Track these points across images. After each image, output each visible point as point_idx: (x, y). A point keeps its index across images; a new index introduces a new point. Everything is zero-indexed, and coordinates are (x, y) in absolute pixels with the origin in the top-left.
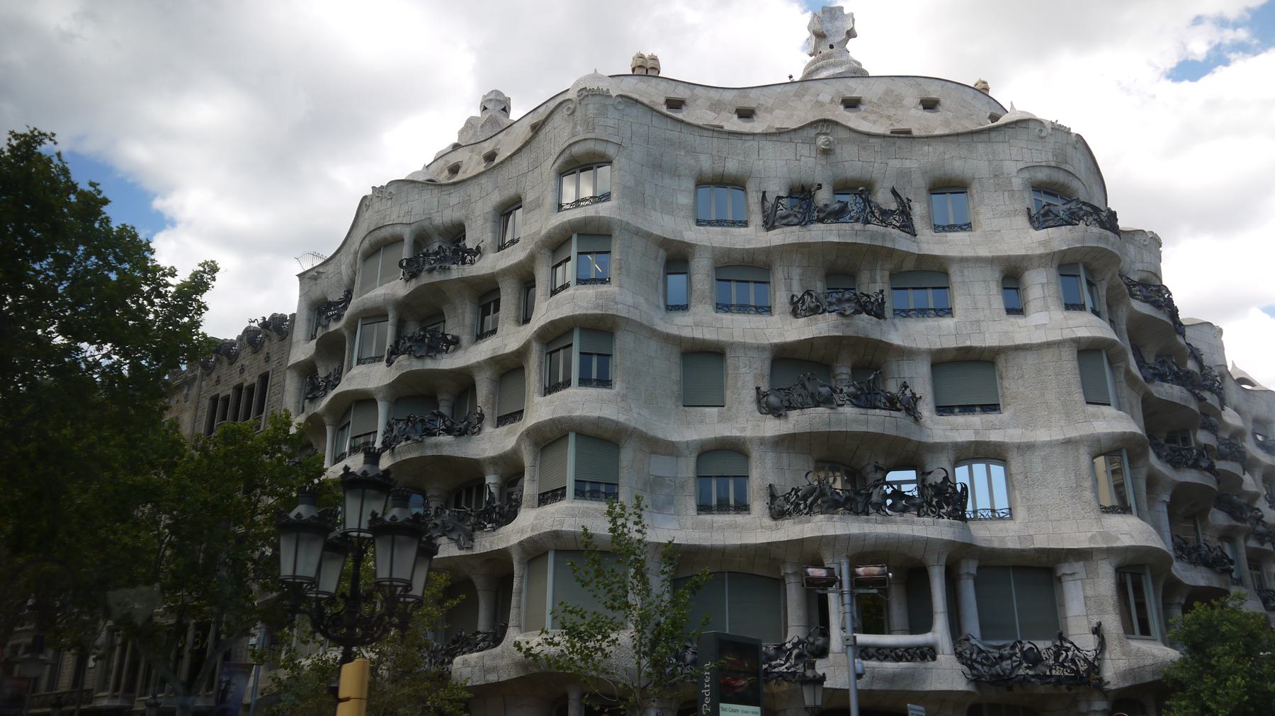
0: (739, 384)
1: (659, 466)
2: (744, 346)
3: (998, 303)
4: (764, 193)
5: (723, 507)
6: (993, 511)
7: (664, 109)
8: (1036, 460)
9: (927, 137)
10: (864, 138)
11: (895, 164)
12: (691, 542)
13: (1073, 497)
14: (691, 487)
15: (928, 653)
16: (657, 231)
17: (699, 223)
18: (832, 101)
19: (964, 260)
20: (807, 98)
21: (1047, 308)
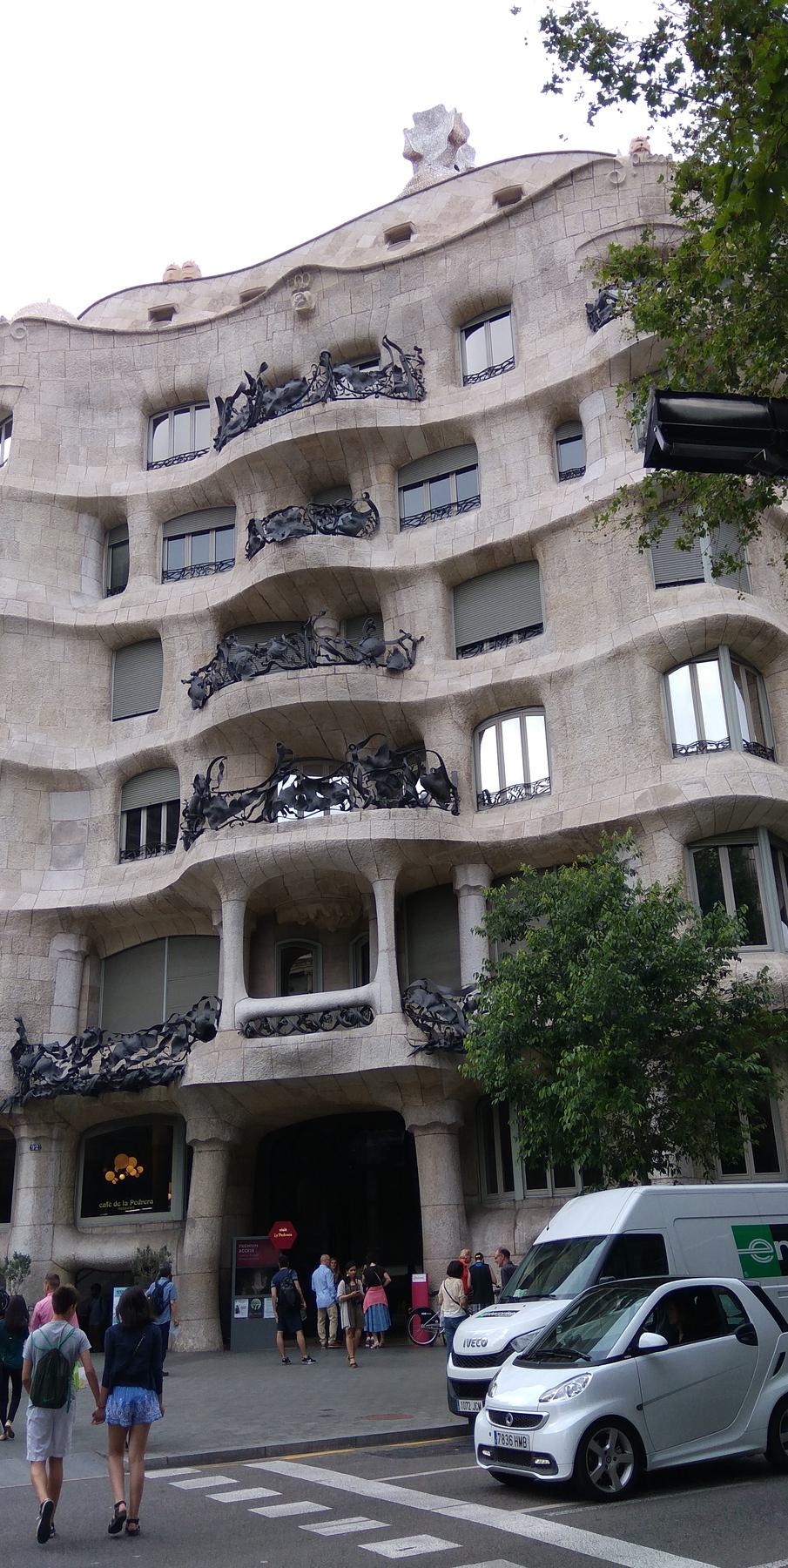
0: (175, 675)
1: (66, 807)
2: (178, 621)
3: (542, 464)
4: (219, 400)
5: (154, 848)
6: (527, 786)
7: (148, 326)
8: (575, 696)
9: (443, 246)
10: (358, 277)
11: (400, 301)
12: (87, 903)
13: (626, 741)
14: (108, 827)
15: (361, 1014)
16: (68, 490)
17: (150, 466)
18: (376, 242)
19: (488, 416)
20: (344, 249)
21: (603, 453)
